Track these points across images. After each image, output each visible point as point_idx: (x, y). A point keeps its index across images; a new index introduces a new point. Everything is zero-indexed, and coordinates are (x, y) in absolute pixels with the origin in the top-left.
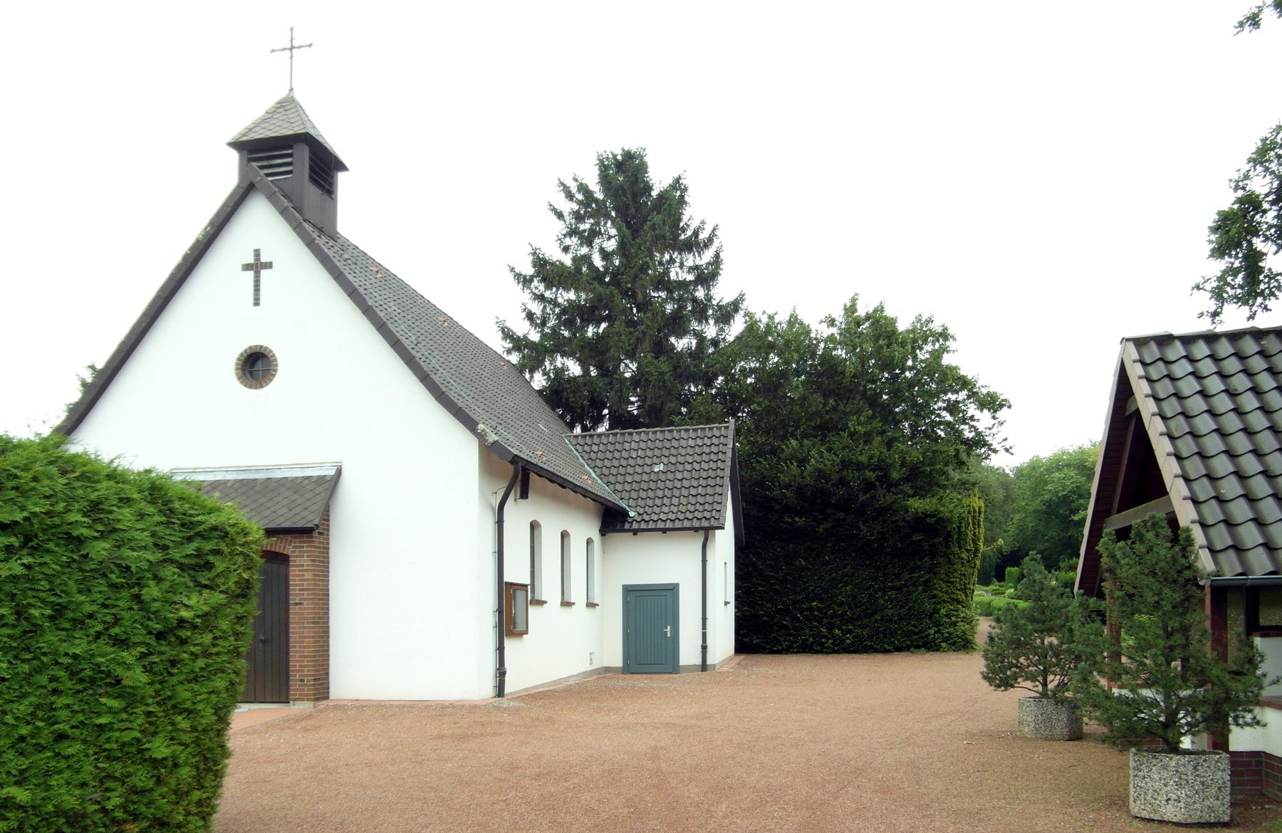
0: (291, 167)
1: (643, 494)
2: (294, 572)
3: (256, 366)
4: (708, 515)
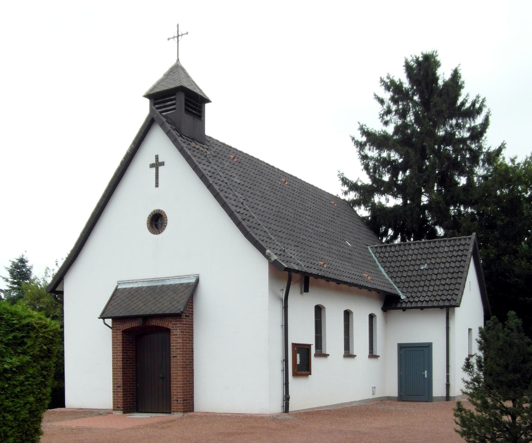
0: (177, 106)
1: (412, 284)
2: (173, 338)
3: (157, 221)
4: (449, 297)
